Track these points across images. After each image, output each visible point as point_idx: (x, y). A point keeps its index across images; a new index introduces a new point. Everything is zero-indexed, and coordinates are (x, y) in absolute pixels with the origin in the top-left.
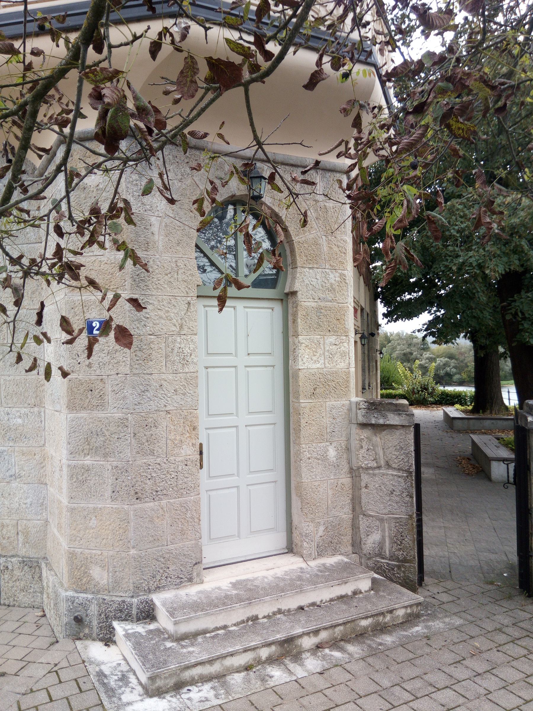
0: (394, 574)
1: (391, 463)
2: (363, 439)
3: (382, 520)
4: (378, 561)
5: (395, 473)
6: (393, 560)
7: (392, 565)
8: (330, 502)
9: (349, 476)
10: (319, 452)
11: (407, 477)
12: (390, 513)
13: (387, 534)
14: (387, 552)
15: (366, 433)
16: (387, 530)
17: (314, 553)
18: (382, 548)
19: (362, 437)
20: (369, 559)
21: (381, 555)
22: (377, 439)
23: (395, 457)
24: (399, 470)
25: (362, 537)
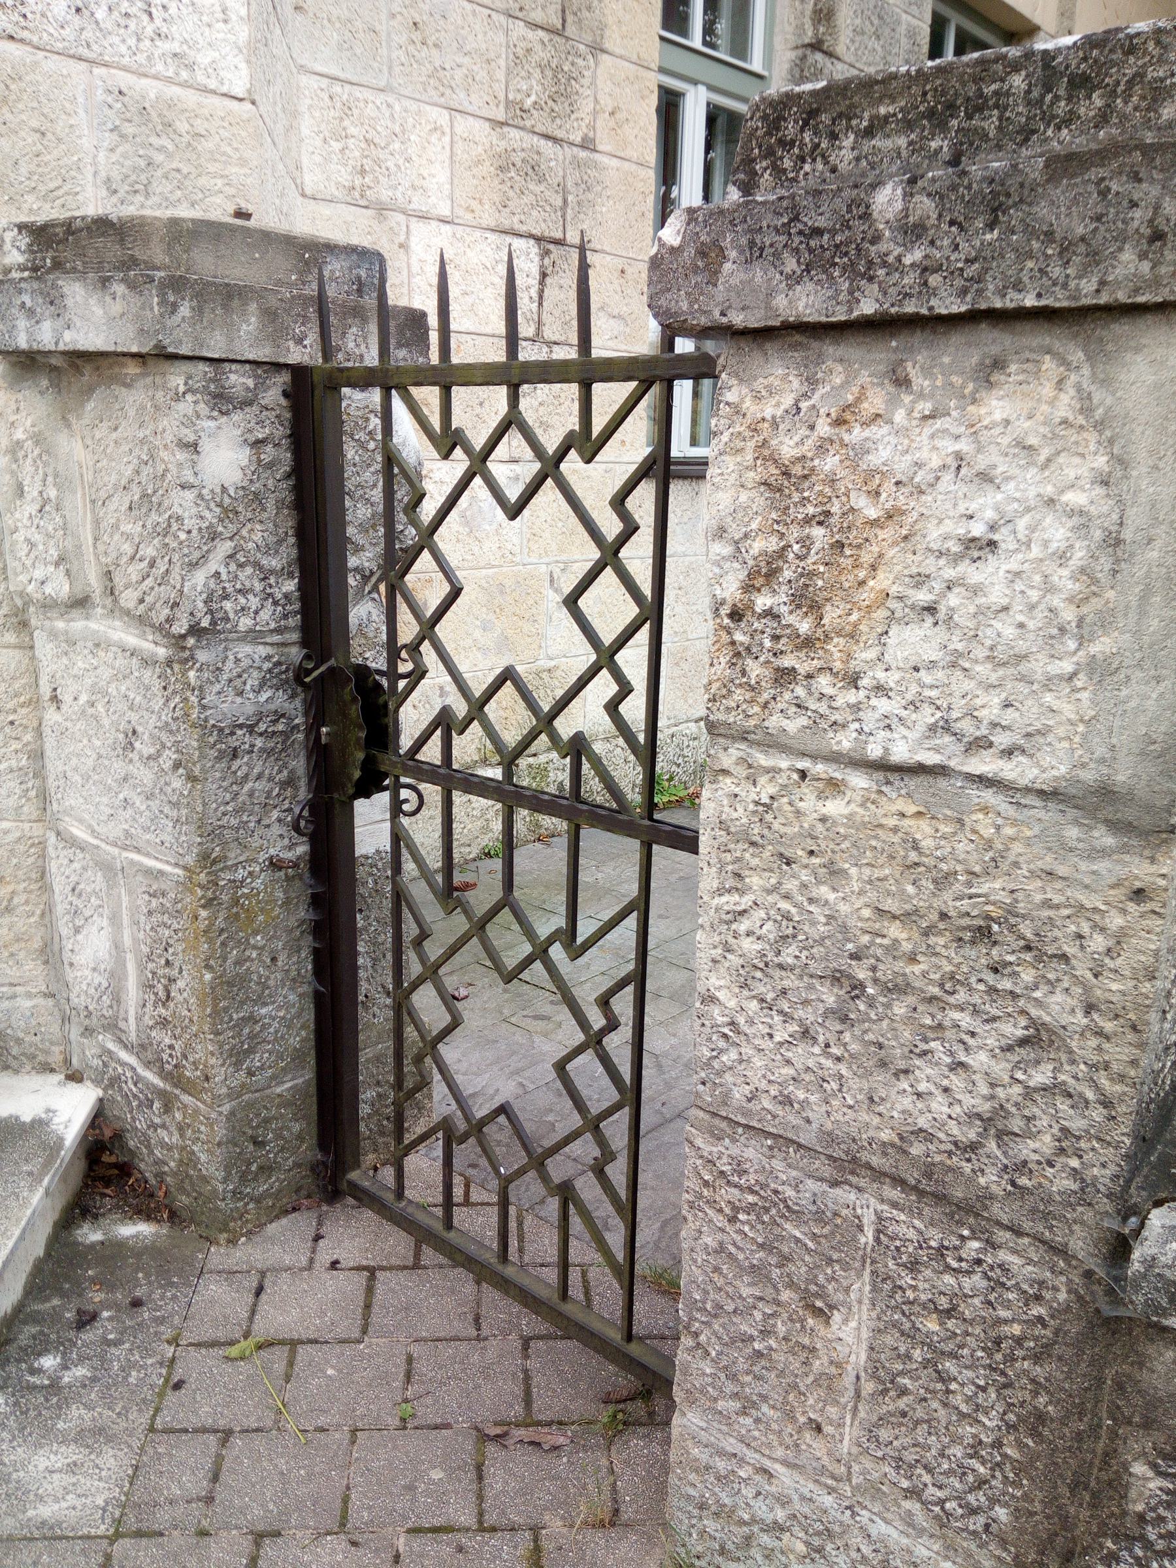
1: (119, 581)
2: (19, 444)
3: (108, 868)
4: (110, 1052)
6: (148, 1064)
9: (10, 638)
11: (169, 663)
12: (127, 843)
14: (132, 1020)
18: (117, 999)
19: (19, 435)
20: (88, 1031)
21: (113, 1026)
23: (128, 549)
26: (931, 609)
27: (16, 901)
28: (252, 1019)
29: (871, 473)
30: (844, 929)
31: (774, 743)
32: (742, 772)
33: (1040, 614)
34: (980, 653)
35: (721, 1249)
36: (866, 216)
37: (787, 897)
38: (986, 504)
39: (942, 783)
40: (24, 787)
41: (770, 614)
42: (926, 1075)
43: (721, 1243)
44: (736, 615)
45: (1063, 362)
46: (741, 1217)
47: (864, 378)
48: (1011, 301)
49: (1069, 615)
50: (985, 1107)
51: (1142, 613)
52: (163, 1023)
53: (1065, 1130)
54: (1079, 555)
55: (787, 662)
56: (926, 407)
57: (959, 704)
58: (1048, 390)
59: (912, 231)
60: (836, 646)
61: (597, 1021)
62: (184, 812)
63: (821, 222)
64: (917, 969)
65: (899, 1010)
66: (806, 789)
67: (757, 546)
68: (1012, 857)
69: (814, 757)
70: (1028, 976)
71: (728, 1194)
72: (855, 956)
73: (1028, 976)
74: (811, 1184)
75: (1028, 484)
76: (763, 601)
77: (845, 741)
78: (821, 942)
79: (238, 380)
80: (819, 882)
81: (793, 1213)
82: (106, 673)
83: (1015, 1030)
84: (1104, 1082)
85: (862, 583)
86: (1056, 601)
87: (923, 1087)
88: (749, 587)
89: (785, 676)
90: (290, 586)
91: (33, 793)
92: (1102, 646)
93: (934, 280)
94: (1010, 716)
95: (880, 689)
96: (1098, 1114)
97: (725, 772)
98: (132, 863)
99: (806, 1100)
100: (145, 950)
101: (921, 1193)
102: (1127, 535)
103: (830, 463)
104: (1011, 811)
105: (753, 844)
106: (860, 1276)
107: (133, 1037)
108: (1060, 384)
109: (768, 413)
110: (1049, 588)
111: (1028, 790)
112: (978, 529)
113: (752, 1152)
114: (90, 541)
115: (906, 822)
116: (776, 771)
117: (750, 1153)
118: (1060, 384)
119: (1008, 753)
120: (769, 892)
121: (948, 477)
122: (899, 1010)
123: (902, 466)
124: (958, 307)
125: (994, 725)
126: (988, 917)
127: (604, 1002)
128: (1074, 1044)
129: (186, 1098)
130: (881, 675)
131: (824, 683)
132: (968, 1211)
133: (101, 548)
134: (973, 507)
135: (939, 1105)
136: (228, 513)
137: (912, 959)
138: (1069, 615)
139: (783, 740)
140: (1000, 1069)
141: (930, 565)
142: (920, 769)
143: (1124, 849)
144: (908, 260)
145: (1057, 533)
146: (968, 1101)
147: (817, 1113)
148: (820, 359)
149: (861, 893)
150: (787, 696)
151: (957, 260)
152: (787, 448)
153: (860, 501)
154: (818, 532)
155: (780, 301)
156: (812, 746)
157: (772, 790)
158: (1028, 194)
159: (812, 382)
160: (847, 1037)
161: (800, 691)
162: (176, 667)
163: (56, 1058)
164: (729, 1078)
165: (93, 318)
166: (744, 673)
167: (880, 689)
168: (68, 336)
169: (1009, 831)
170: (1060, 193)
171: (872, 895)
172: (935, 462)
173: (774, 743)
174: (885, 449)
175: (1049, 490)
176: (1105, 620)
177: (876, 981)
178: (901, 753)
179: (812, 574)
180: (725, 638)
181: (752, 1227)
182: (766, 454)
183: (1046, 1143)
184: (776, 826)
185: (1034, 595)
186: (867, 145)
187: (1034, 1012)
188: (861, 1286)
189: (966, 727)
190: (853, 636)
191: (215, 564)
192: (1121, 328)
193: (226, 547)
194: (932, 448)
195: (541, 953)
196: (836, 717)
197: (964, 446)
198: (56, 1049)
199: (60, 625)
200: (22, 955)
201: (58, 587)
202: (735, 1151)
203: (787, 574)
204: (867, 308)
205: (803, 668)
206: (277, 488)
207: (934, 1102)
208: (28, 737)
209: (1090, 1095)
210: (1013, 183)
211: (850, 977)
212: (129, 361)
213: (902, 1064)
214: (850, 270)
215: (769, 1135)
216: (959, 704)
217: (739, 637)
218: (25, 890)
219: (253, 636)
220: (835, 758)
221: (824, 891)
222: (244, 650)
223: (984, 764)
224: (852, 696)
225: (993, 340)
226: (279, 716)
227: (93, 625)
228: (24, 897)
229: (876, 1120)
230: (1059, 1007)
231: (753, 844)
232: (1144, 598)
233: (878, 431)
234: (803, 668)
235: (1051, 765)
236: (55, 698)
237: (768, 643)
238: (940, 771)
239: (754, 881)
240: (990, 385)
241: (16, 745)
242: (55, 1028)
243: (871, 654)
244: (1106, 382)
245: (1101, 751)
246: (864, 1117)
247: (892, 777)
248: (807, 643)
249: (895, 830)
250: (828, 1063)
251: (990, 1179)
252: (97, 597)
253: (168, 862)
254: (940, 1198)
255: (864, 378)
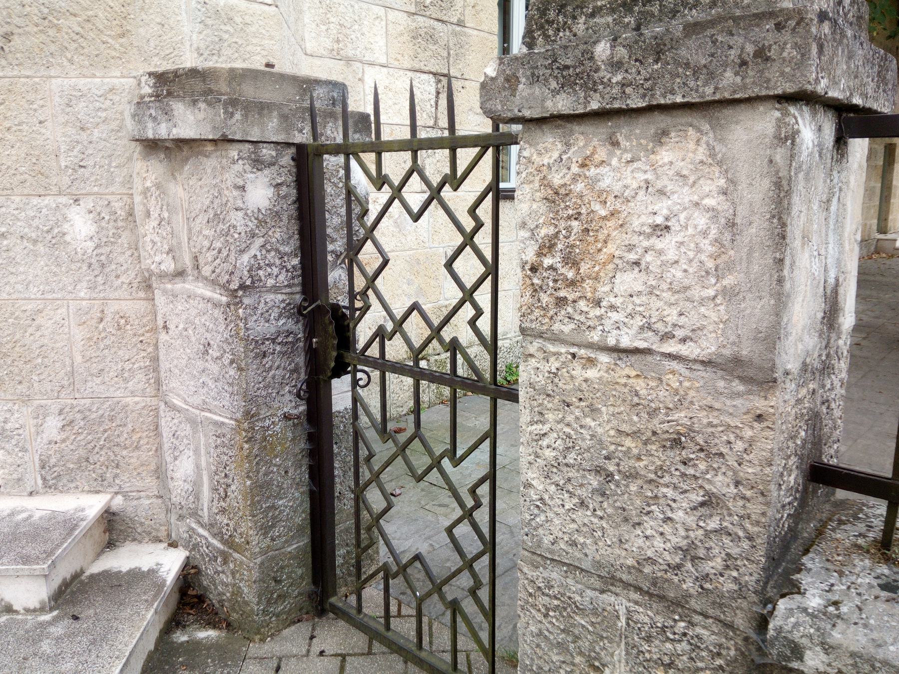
0: (217, 572)
1: (201, 261)
4: (193, 529)
5: (208, 293)
6: (214, 536)
7: (214, 548)
8: (78, 359)
9: (142, 294)
10: (36, 222)
11: (228, 305)
13: (203, 464)
15: (149, 172)
16: (203, 451)
17: (34, 479)
18: (197, 498)
19: (148, 184)
20: (181, 517)
22: (177, 191)
23: (206, 243)
24: (214, 283)
25: (169, 459)
26: (637, 263)
27: (141, 442)
28: (273, 507)
29: (602, 192)
30: (600, 442)
31: (557, 339)
32: (540, 355)
33: (695, 264)
34: (665, 286)
35: (540, 633)
36: (592, 58)
37: (568, 425)
38: (663, 207)
39: (649, 358)
40: (147, 377)
41: (551, 268)
42: (650, 526)
43: (540, 630)
44: (534, 269)
45: (699, 130)
46: (551, 613)
47: (595, 142)
48: (669, 100)
49: (710, 264)
50: (684, 543)
51: (749, 262)
52: (223, 511)
53: (728, 554)
54: (713, 233)
55: (562, 294)
56: (628, 156)
57: (655, 314)
58: (692, 146)
59: (616, 65)
60: (588, 285)
61: (470, 503)
62: (236, 388)
63: (569, 62)
64: (642, 464)
65: (633, 488)
66: (576, 364)
67: (543, 232)
68: (689, 399)
69: (579, 346)
70: (702, 466)
71: (543, 600)
72: (607, 458)
73: (702, 466)
74: (589, 592)
75: (684, 195)
76: (547, 261)
77: (595, 337)
78: (588, 450)
79: (267, 152)
80: (585, 416)
81: (580, 610)
82: (194, 312)
83: (697, 497)
84: (748, 526)
85: (600, 250)
86: (703, 257)
87: (649, 532)
88: (540, 254)
89: (561, 302)
90: (296, 261)
91: (152, 381)
92: (729, 280)
93: (628, 90)
94: (682, 320)
95: (612, 307)
96: (746, 544)
97: (531, 355)
98: (207, 418)
99: (584, 543)
100: (214, 468)
101: (651, 595)
102: (738, 220)
103: (579, 187)
104: (687, 373)
105: (548, 395)
106: (619, 646)
107: (206, 520)
108: (698, 142)
109: (546, 162)
110: (699, 250)
111: (695, 361)
112: (659, 220)
113: (555, 575)
114: (186, 240)
115: (631, 381)
116: (558, 354)
117: (554, 575)
118: (698, 142)
119: (684, 340)
120: (558, 422)
121: (642, 193)
122: (633, 488)
123: (617, 188)
124: (641, 104)
125: (675, 325)
126: (679, 433)
127: (473, 491)
128: (730, 505)
129: (236, 555)
130: (612, 300)
131: (582, 304)
132: (677, 605)
133: (192, 243)
134: (656, 208)
135: (658, 543)
136: (261, 223)
137: (639, 459)
138: (710, 264)
139: (562, 337)
140: (691, 520)
141: (635, 239)
142: (636, 351)
143: (749, 392)
144: (614, 80)
145: (701, 220)
146: (675, 540)
147: (590, 550)
148: (572, 133)
149: (609, 421)
150: (563, 312)
151: (640, 80)
152: (557, 180)
153: (596, 207)
154: (575, 224)
155: (549, 104)
156: (578, 340)
157: (557, 365)
158: (675, 43)
159: (568, 145)
160: (605, 505)
161: (570, 310)
162: (232, 307)
163: (163, 534)
164: (541, 531)
165: (188, 121)
166: (539, 300)
167: (612, 307)
168: (175, 131)
169: (687, 384)
170: (691, 43)
171: (615, 422)
172: (635, 185)
173: (557, 339)
174: (608, 179)
175: (695, 198)
176: (730, 267)
177: (619, 471)
178: (626, 342)
179: (573, 246)
180: (528, 282)
181: (557, 620)
182: (545, 183)
183: (718, 563)
184: (560, 385)
185: (691, 254)
186: (592, 22)
187: (707, 487)
188: (620, 652)
189: (659, 326)
190: (596, 278)
191: (254, 251)
192: (728, 112)
193: (259, 241)
194: (633, 178)
195: (436, 464)
196: (590, 323)
197: (649, 176)
198: (163, 528)
199: (169, 286)
200: (144, 474)
201: (169, 266)
202: (546, 574)
203: (560, 246)
204: (594, 106)
205: (571, 297)
206: (289, 209)
207: (655, 541)
208: (150, 349)
209: (741, 534)
210: (667, 39)
211: (605, 470)
212: (208, 143)
213: (636, 520)
214: (584, 86)
215: (565, 564)
216: (655, 314)
217: (536, 281)
218: (147, 437)
219: (275, 289)
220: (590, 346)
221: (588, 421)
222: (270, 297)
223: (671, 347)
224: (598, 312)
225: (661, 120)
226: (289, 333)
227: (187, 286)
228: (146, 440)
229: (624, 553)
230: (721, 484)
231: (548, 395)
232: (750, 254)
233: (603, 170)
234: (571, 297)
235: (706, 347)
236: (165, 327)
237: (551, 284)
238: (647, 352)
239: (550, 416)
240: (661, 144)
241: (143, 354)
242: (162, 516)
243: (607, 288)
244: (722, 140)
245: (733, 338)
246: (617, 551)
247: (622, 355)
248: (572, 283)
249: (625, 385)
250: (595, 520)
251: (689, 585)
252: (189, 271)
253: (226, 417)
254: (662, 598)
255: (595, 142)
